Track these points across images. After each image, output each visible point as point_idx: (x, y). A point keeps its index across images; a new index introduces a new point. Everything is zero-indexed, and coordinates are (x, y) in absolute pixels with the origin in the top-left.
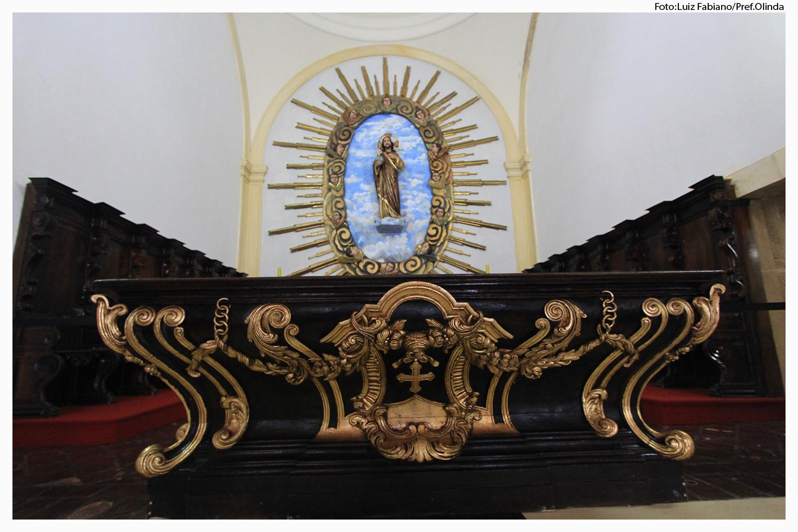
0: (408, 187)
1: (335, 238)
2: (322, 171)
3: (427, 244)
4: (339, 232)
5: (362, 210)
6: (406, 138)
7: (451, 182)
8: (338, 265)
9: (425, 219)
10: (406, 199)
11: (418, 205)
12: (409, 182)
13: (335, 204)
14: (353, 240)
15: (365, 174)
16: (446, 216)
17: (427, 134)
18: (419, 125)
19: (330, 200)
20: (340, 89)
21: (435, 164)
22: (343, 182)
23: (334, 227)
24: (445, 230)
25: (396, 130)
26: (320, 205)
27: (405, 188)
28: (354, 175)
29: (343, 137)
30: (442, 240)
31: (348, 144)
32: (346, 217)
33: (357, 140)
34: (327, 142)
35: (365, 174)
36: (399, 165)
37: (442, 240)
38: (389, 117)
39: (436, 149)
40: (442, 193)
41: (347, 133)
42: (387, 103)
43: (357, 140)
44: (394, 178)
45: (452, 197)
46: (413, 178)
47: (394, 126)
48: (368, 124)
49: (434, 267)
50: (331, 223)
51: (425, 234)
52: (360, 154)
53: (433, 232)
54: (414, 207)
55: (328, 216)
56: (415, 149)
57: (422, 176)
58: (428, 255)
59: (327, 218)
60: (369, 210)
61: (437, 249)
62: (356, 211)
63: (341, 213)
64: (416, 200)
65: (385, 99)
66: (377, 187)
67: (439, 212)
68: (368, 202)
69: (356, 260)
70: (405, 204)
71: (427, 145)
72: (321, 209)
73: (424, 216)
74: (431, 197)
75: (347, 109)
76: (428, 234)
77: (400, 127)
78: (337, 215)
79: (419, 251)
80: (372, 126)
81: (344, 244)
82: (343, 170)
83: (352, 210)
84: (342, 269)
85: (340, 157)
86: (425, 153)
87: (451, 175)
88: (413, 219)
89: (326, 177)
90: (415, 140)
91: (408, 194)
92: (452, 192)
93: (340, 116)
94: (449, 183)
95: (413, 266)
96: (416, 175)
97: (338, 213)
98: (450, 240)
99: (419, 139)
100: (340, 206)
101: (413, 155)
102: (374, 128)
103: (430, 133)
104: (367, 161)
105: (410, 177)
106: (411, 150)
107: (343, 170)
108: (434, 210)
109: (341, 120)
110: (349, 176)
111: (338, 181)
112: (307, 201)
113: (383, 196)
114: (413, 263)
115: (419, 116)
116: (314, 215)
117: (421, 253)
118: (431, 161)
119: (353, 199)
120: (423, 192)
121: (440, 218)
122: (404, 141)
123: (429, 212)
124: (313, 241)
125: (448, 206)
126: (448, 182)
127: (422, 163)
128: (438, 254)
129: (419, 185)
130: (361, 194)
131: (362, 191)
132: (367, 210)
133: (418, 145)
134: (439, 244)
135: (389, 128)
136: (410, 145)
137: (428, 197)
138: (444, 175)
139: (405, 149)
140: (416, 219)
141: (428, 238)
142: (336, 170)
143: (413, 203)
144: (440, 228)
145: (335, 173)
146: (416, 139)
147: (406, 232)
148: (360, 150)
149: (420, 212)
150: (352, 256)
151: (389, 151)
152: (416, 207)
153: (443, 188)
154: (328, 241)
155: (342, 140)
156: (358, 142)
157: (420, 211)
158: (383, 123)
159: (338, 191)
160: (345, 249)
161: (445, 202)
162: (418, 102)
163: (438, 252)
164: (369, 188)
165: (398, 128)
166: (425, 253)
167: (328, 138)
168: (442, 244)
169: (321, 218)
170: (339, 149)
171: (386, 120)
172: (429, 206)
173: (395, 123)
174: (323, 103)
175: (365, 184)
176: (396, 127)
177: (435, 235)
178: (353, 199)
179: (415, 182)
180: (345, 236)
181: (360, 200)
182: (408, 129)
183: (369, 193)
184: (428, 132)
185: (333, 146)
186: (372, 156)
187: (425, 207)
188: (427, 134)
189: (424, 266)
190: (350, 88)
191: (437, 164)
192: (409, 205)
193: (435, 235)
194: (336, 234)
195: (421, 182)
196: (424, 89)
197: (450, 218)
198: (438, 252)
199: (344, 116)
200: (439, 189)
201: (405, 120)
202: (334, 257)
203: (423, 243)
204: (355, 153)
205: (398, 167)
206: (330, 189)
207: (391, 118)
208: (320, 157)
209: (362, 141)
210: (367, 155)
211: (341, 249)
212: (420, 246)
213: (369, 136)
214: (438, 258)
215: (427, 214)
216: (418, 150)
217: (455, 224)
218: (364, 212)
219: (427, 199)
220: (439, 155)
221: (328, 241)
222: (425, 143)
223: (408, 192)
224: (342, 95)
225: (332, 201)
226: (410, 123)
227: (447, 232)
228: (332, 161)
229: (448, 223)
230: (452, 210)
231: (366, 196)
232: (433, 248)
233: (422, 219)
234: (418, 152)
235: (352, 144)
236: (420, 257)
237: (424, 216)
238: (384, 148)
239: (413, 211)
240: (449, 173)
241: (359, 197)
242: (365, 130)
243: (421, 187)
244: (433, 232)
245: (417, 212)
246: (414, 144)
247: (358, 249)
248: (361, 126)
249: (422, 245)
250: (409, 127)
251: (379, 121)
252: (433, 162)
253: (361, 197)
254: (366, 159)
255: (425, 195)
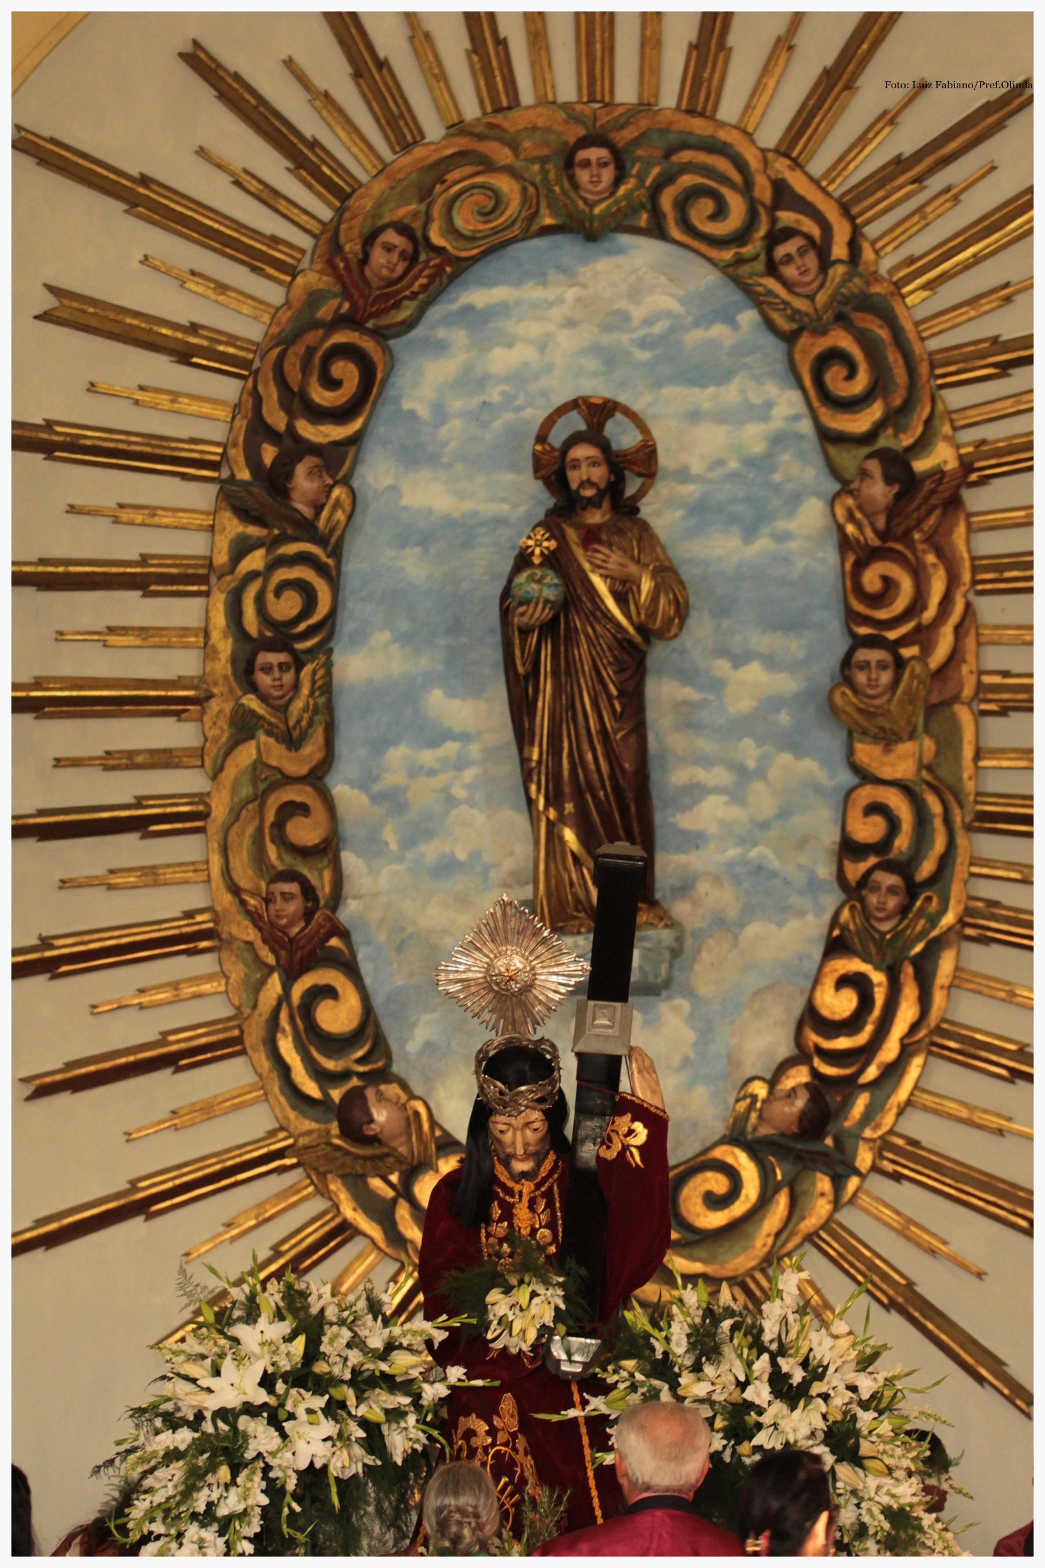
0: (705, 715)
1: (273, 1025)
2: (198, 602)
3: (799, 1076)
4: (298, 991)
5: (431, 851)
6: (703, 397)
7: (968, 691)
8: (295, 1176)
9: (801, 913)
10: (695, 793)
11: (764, 825)
12: (718, 685)
13: (279, 825)
14: (380, 1047)
15: (455, 628)
16: (921, 913)
17: (834, 376)
18: (791, 318)
19: (246, 791)
20: (303, 61)
21: (871, 579)
22: (326, 687)
23: (271, 959)
24: (910, 993)
25: (643, 344)
26: (191, 819)
27: (688, 720)
28: (386, 636)
29: (322, 396)
30: (890, 1050)
31: (355, 440)
32: (337, 897)
33: (407, 405)
34: (224, 413)
35: (455, 628)
36: (652, 613)
37: (890, 1050)
38: (609, 253)
39: (879, 490)
40: (901, 762)
41: (346, 370)
42: (595, 173)
43: (407, 405)
44: (622, 694)
45: (970, 786)
46: (739, 660)
47: (638, 313)
48: (477, 296)
49: (837, 1204)
50: (251, 934)
51: (798, 1007)
52: (428, 495)
53: (839, 1004)
54: (741, 841)
55: (235, 890)
56: (759, 465)
57: (794, 646)
58: (800, 1146)
59: (226, 899)
60: (476, 854)
61: (861, 1102)
62: (399, 859)
63: (312, 878)
64: (748, 797)
65: (582, 155)
66: (523, 736)
67: (876, 888)
68: (471, 802)
69: (400, 1160)
70: (684, 821)
71: (832, 450)
72: (196, 839)
73: (794, 900)
74: (846, 778)
75: (341, 192)
76: (812, 1017)
77: (669, 314)
78: (286, 897)
79: (754, 1116)
80: (503, 309)
81: (330, 1065)
82: (323, 609)
83: (374, 848)
84: (319, 1205)
85: (307, 529)
86: (818, 495)
87: (970, 642)
88: (732, 913)
89: (225, 647)
90: (764, 411)
91: (706, 762)
92: (968, 752)
93: (305, 241)
94: (956, 698)
95: (714, 1202)
96: (761, 641)
97: (293, 888)
98: (934, 1050)
99: (788, 404)
100: (305, 832)
101: (740, 508)
102: (511, 326)
103: (852, 375)
104: (468, 543)
105: (723, 652)
106: (734, 476)
107: (323, 609)
108: (855, 870)
109: (311, 278)
110: (359, 639)
111: (296, 687)
112: (116, 791)
113: (554, 799)
114: (718, 1183)
115: (790, 271)
116: (151, 876)
117: (764, 1131)
118: (858, 556)
119: (376, 787)
120: (794, 745)
121: (885, 927)
122: (695, 416)
123: (825, 871)
124: (153, 1036)
125: (940, 844)
126: (947, 695)
127: (801, 563)
128: (868, 1133)
129: (772, 703)
130: (428, 757)
131: (435, 735)
132: (462, 855)
133: (779, 440)
134: (872, 1073)
135: (606, 327)
136: (735, 443)
137: (822, 776)
138: (927, 650)
139: (697, 467)
140: (749, 912)
141: (813, 1038)
142: (286, 607)
143: (736, 813)
144: (878, 978)
145: (280, 636)
146: (769, 405)
147: (689, 992)
148: (425, 473)
149: (773, 874)
150: (374, 1140)
151: (595, 517)
152: (755, 844)
153: (912, 735)
154: (239, 1040)
155: (320, 415)
156: (412, 413)
157: (775, 864)
158: (571, 294)
159: (292, 741)
160: (336, 1094)
161: (922, 817)
162: (784, 150)
163: (868, 1117)
164: (475, 714)
165: (658, 328)
166: (783, 1135)
167: (230, 389)
168: (894, 1071)
169: (194, 897)
170: (304, 481)
171: (585, 272)
172: (831, 837)
173: (647, 282)
174: (202, 152)
175: (451, 693)
176: (649, 321)
177: (851, 1024)
178: (376, 787)
179: (749, 685)
180: (338, 1017)
181: (423, 795)
182: (718, 331)
183: (474, 750)
184: (844, 372)
185: (269, 453)
186: (502, 509)
187: (804, 842)
188: (834, 376)
189: (782, 1200)
190: (356, 986)
191: (888, 582)
192: (713, 829)
193: (851, 1024)
194: (286, 996)
195: (786, 684)
196: (829, 59)
197: (949, 919)
198: (868, 1117)
199: (330, 239)
200: (888, 739)
201: (703, 278)
202: (272, 1133)
203: (784, 1067)
204: (393, 489)
205: (641, 629)
206: (244, 727)
207: (619, 259)
208: (183, 518)
209: (440, 413)
210: (468, 505)
211: (311, 1089)
212: (760, 1090)
213: (483, 381)
214: (864, 1158)
215: (813, 885)
216: (777, 477)
217: (974, 949)
218: (447, 867)
219: (819, 790)
220: (907, 508)
221: (239, 1040)
222: (827, 437)
223: (705, 745)
224: (325, 101)
225: (261, 798)
226: (737, 296)
227: (925, 1001)
228: (258, 544)
229: (935, 947)
230: (961, 869)
231: (460, 764)
232: (834, 1099)
233: (782, 913)
234: (777, 488)
235: (381, 429)
236: (755, 1149)
237: (794, 900)
238: (565, 503)
239: (731, 865)
240: (959, 630)
241: (415, 771)
242: (459, 336)
243: (784, 718)
244: (839, 1004)
245: (759, 869)
246: (754, 437)
247: (412, 1096)
248: (435, 313)
249: (772, 1083)
250: (731, 321)
251: (543, 280)
252: (860, 566)
253: (431, 773)
254: (462, 532)
255: (809, 765)
